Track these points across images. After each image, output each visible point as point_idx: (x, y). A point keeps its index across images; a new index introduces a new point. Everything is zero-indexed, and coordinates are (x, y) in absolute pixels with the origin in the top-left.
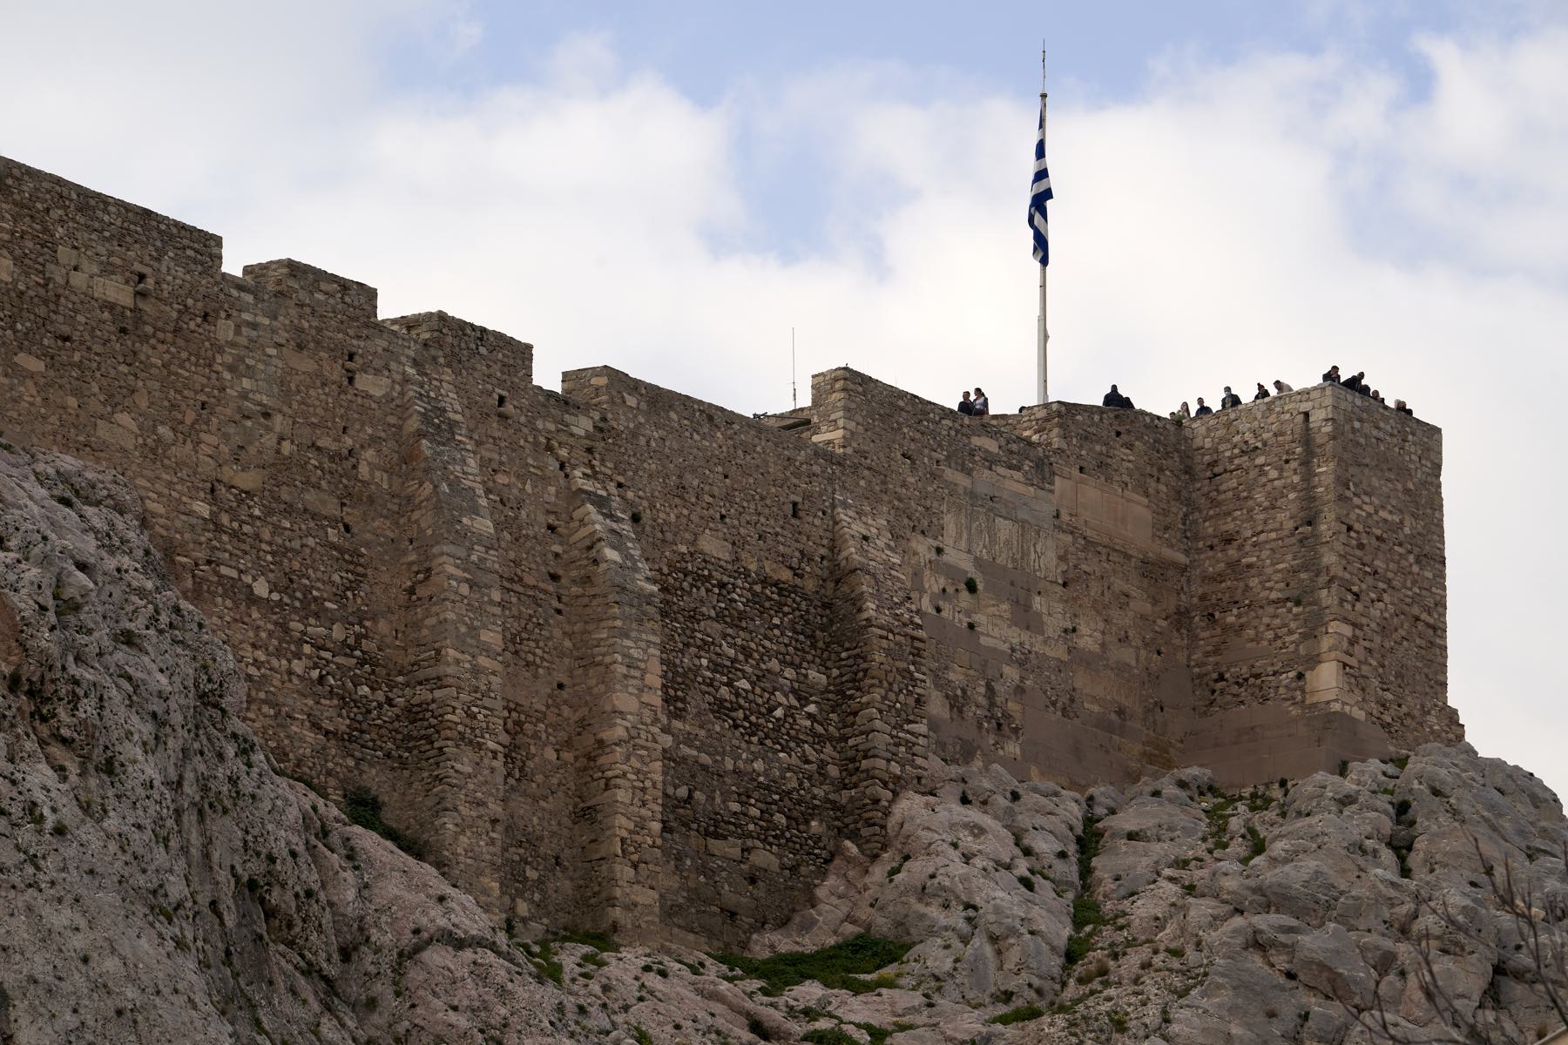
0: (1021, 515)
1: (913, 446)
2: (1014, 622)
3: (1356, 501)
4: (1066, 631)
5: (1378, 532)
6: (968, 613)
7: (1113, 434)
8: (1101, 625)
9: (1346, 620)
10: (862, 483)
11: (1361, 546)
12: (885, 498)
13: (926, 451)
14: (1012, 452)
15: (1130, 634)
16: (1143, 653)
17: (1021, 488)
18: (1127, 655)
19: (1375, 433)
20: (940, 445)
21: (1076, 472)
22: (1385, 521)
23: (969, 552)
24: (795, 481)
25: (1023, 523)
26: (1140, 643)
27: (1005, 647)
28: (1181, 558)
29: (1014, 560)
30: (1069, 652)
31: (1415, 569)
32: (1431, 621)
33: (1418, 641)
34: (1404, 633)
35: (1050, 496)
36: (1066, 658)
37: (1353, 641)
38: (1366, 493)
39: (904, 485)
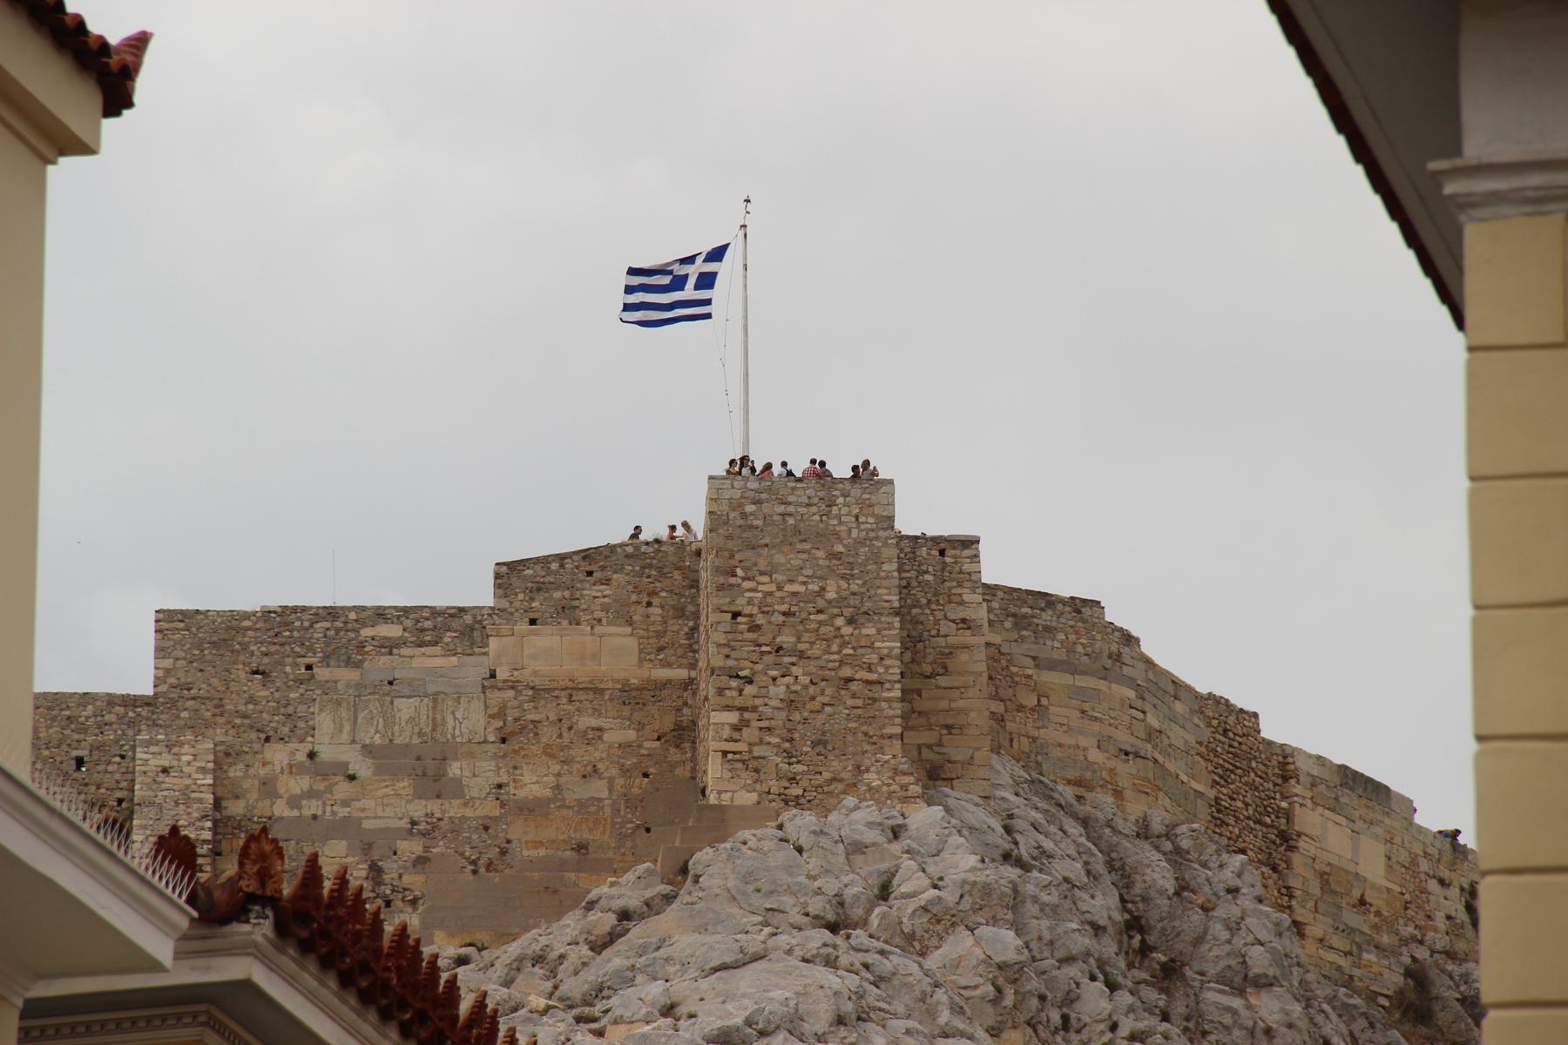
0: (431, 689)
1: (266, 660)
2: (419, 795)
3: (747, 584)
4: (500, 786)
5: (784, 608)
6: (345, 803)
7: (581, 576)
8: (556, 768)
9: (728, 708)
10: (184, 714)
11: (754, 628)
12: (220, 720)
13: (289, 660)
14: (422, 630)
15: (600, 766)
16: (620, 782)
17: (439, 662)
18: (598, 789)
19: (781, 509)
20: (311, 649)
21: (523, 626)
22: (795, 594)
23: (354, 742)
24: (76, 737)
25: (436, 698)
26: (614, 772)
27: (404, 824)
28: (683, 673)
29: (420, 734)
30: (503, 805)
31: (847, 630)
32: (874, 677)
33: (850, 702)
34: (826, 700)
35: (484, 658)
36: (497, 812)
37: (737, 728)
38: (762, 573)
39: (252, 700)
